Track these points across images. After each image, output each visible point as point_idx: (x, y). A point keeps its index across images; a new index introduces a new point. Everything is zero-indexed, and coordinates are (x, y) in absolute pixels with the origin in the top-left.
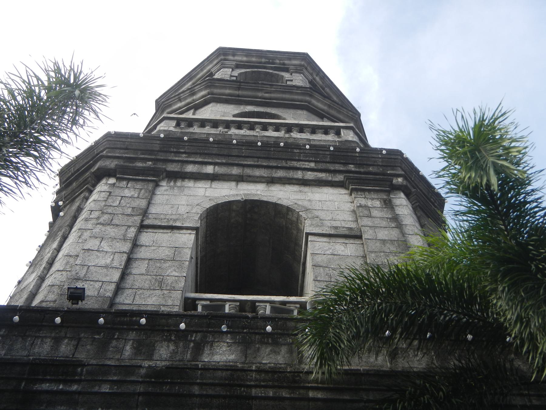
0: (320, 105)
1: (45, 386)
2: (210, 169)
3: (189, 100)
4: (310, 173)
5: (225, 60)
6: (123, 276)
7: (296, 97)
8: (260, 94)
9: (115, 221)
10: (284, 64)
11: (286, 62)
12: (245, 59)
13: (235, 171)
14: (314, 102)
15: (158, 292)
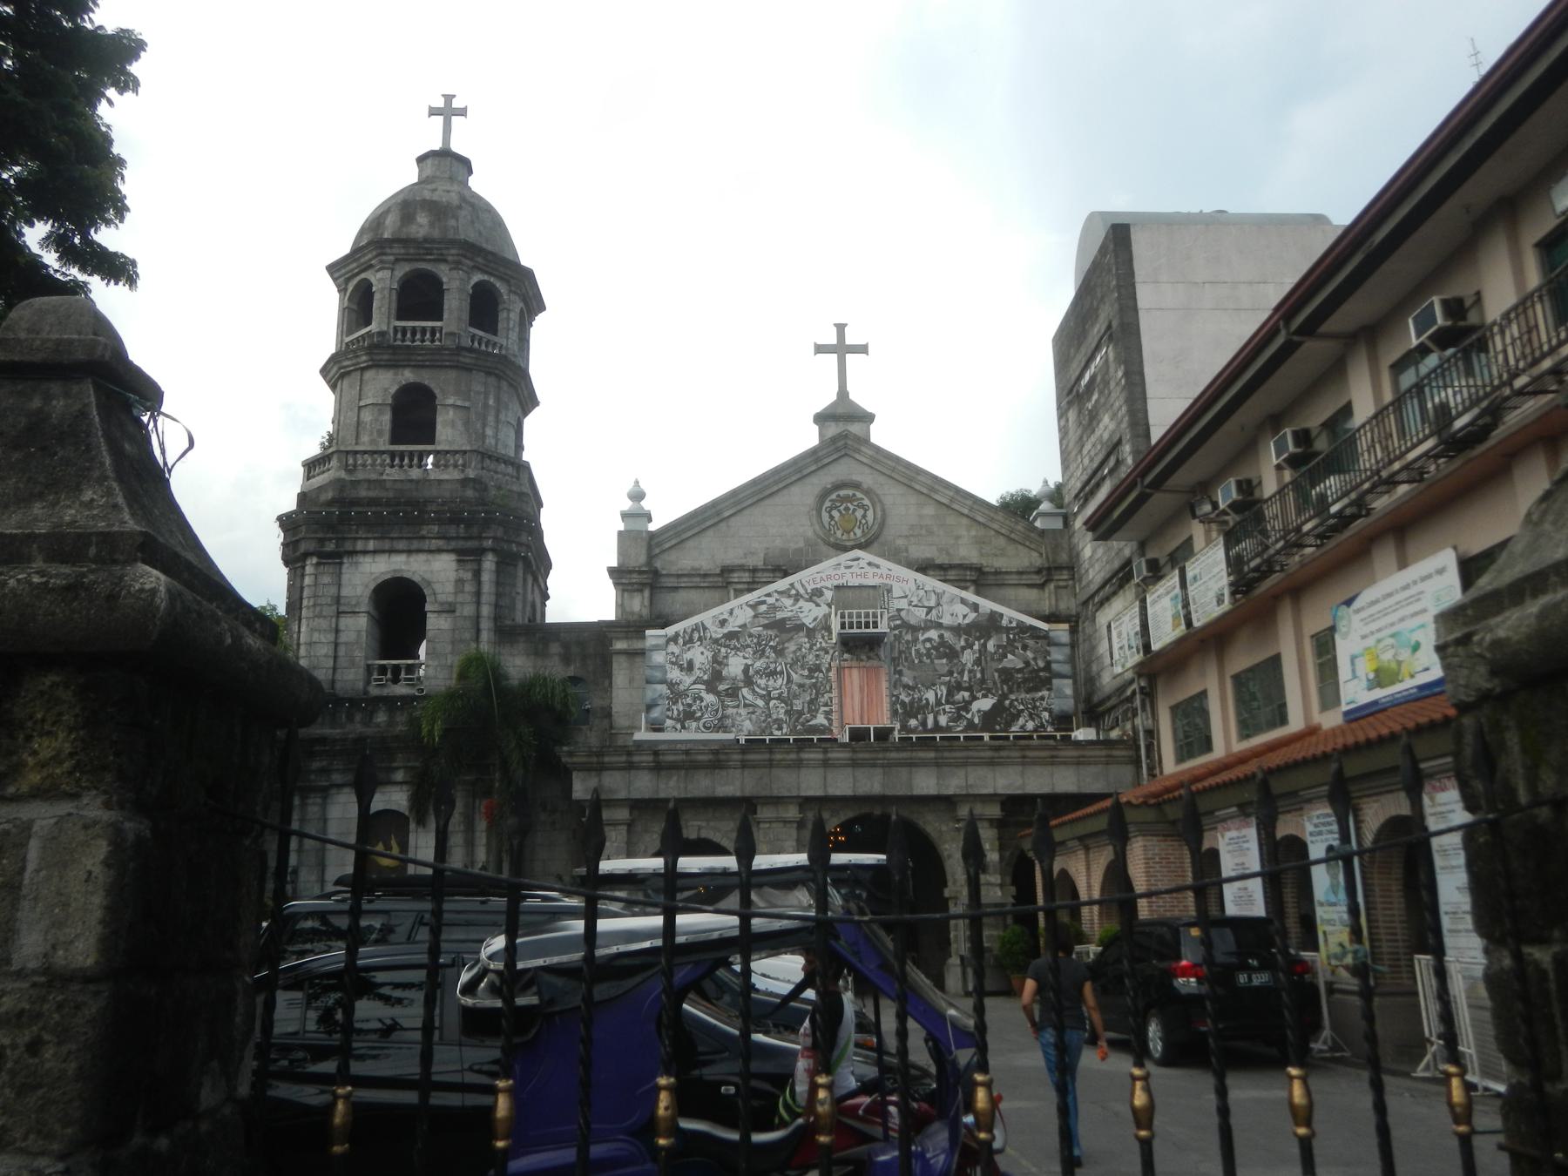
0: (468, 361)
1: (317, 748)
2: (371, 545)
3: (354, 361)
4: (433, 541)
5: (385, 254)
6: (335, 658)
7: (446, 358)
8: (413, 357)
9: (324, 613)
10: (442, 254)
11: (445, 252)
12: (402, 251)
13: (387, 545)
14: (462, 359)
15: (353, 670)
